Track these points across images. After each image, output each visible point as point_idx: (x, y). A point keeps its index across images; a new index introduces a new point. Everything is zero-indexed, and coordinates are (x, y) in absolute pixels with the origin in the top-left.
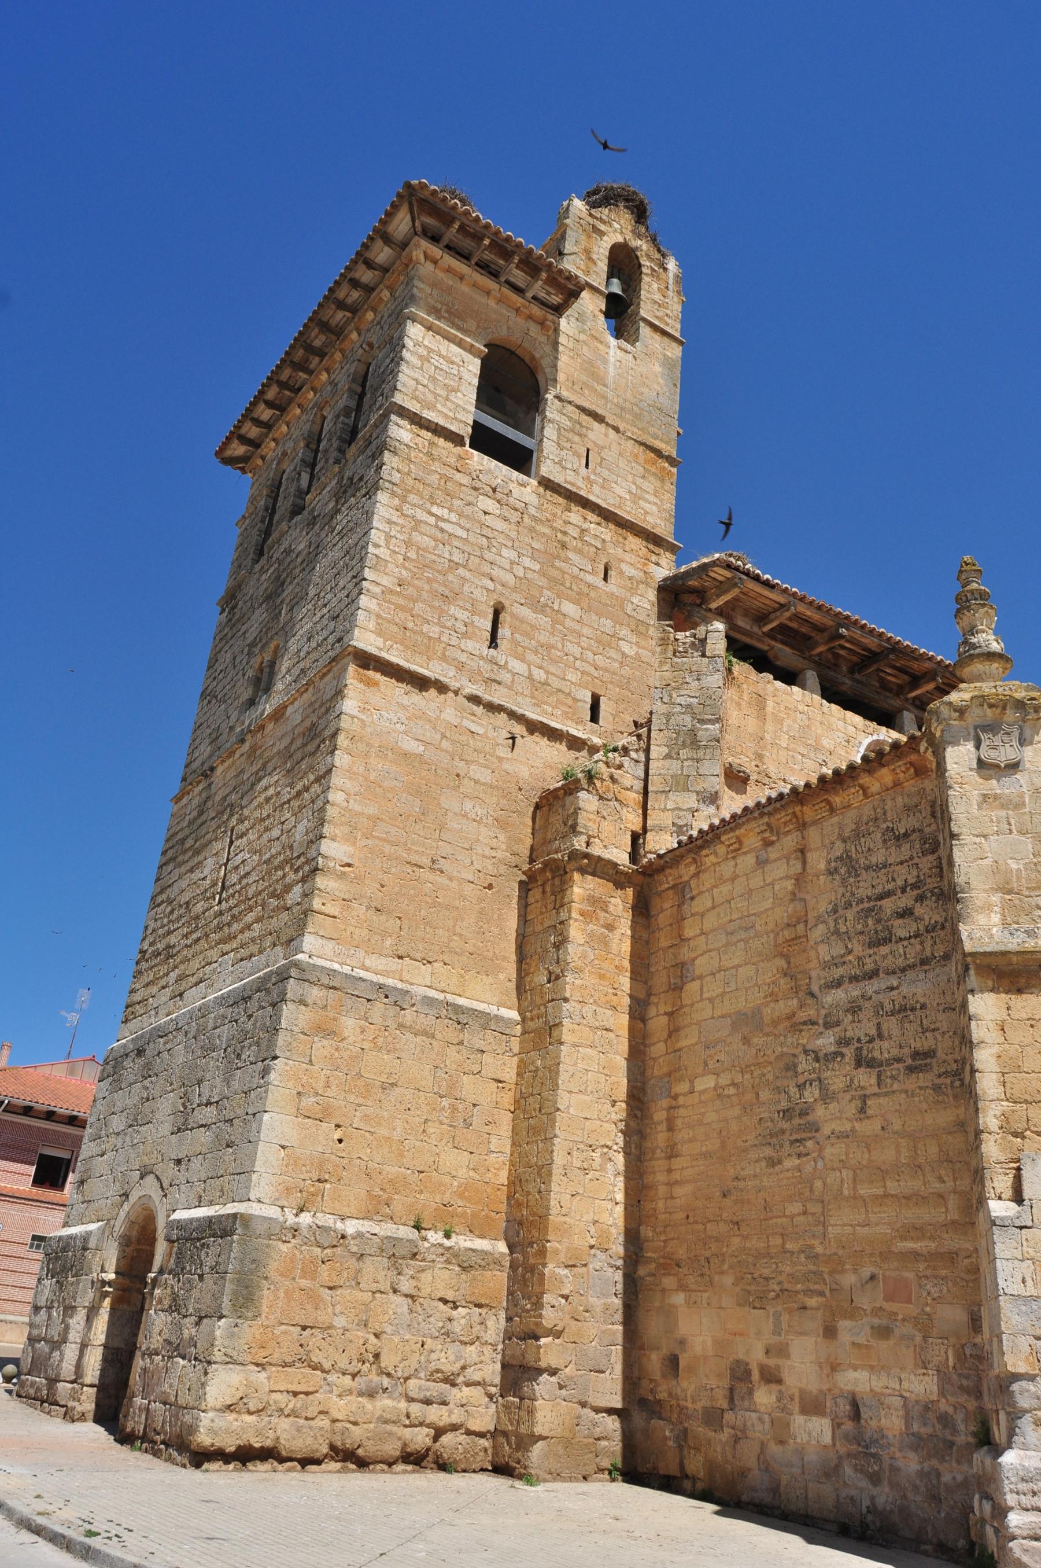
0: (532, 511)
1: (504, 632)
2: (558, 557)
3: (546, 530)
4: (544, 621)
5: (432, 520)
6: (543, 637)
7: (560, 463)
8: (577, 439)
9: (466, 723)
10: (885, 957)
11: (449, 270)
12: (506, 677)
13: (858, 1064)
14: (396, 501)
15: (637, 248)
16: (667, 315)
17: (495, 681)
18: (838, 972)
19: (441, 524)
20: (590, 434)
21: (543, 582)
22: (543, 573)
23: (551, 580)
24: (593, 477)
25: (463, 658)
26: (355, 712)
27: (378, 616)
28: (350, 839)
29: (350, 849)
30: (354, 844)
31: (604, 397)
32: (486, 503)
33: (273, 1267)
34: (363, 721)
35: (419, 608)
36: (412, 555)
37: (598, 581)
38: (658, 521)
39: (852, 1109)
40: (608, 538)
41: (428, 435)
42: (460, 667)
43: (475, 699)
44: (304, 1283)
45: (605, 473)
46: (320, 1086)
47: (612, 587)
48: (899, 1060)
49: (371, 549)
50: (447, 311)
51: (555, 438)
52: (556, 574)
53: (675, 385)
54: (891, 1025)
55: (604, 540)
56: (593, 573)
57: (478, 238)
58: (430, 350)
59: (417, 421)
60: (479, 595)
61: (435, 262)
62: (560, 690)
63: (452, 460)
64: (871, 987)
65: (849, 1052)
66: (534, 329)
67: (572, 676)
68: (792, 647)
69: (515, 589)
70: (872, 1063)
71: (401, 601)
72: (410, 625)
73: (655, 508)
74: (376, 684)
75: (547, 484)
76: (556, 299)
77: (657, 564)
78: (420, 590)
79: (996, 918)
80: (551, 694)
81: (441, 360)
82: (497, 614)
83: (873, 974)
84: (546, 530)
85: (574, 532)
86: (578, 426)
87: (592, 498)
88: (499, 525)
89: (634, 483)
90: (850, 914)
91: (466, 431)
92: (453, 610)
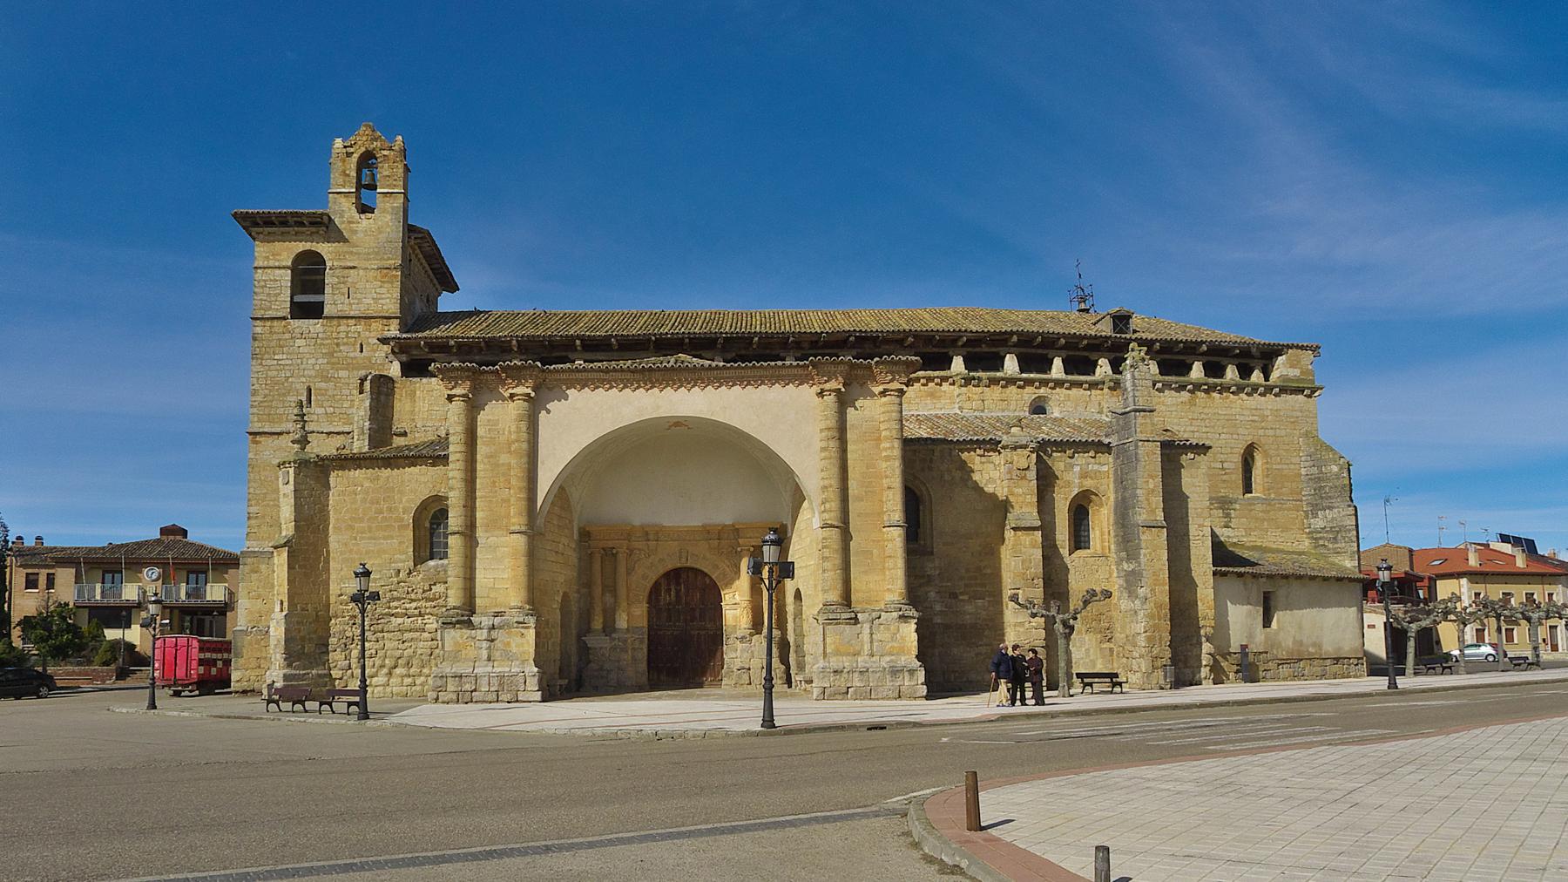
0: (320, 335)
2: (336, 352)
3: (328, 342)
6: (330, 393)
7: (334, 303)
8: (342, 286)
14: (260, 361)
20: (349, 280)
23: (333, 364)
24: (352, 302)
31: (359, 254)
32: (299, 342)
36: (269, 382)
37: (358, 354)
41: (268, 323)
50: (273, 255)
55: (359, 332)
56: (355, 351)
58: (265, 281)
68: (443, 353)
69: (315, 377)
71: (266, 404)
74: (260, 442)
77: (389, 330)
80: (336, 416)
82: (309, 390)
84: (329, 341)
85: (342, 335)
91: (286, 312)
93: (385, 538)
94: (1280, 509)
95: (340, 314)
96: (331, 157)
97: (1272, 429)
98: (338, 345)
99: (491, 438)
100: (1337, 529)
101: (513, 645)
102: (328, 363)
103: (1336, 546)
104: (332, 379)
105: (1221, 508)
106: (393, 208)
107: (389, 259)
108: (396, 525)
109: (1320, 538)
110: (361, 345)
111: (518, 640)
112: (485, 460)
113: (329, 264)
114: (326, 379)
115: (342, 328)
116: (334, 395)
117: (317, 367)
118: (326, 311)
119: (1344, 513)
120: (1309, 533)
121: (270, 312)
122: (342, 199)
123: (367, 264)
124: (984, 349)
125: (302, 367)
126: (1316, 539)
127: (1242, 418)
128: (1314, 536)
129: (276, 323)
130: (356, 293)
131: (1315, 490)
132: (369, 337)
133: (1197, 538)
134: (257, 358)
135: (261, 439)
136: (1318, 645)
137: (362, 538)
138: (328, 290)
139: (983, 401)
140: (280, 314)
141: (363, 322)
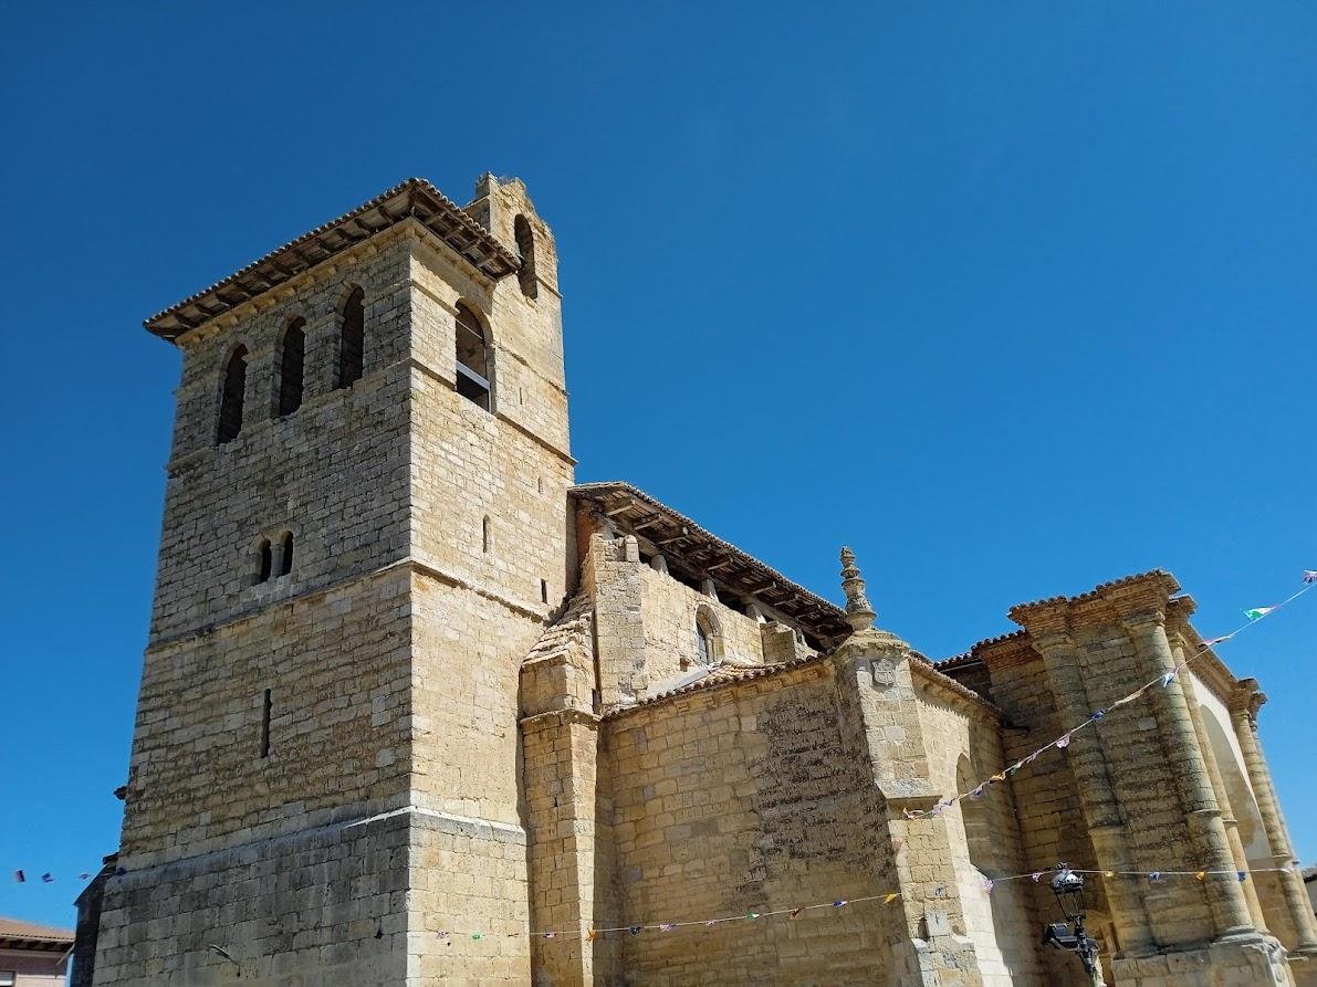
1: (491, 538)
2: (513, 477)
8: (514, 381)
9: (479, 613)
10: (805, 789)
11: (431, 245)
12: (495, 574)
13: (793, 855)
17: (490, 577)
18: (772, 798)
19: (449, 457)
25: (472, 562)
29: (428, 721)
30: (429, 717)
35: (444, 525)
37: (534, 492)
39: (790, 885)
42: (471, 569)
43: (482, 594)
46: (434, 906)
48: (820, 854)
49: (412, 481)
54: (813, 831)
57: (455, 224)
59: (425, 371)
61: (421, 237)
63: (449, 404)
64: (796, 808)
65: (785, 849)
66: (481, 290)
70: (802, 856)
75: (502, 418)
76: (498, 269)
79: (892, 776)
83: (798, 799)
87: (525, 427)
88: (479, 453)
90: (778, 760)
91: (453, 379)
114: (508, 517)
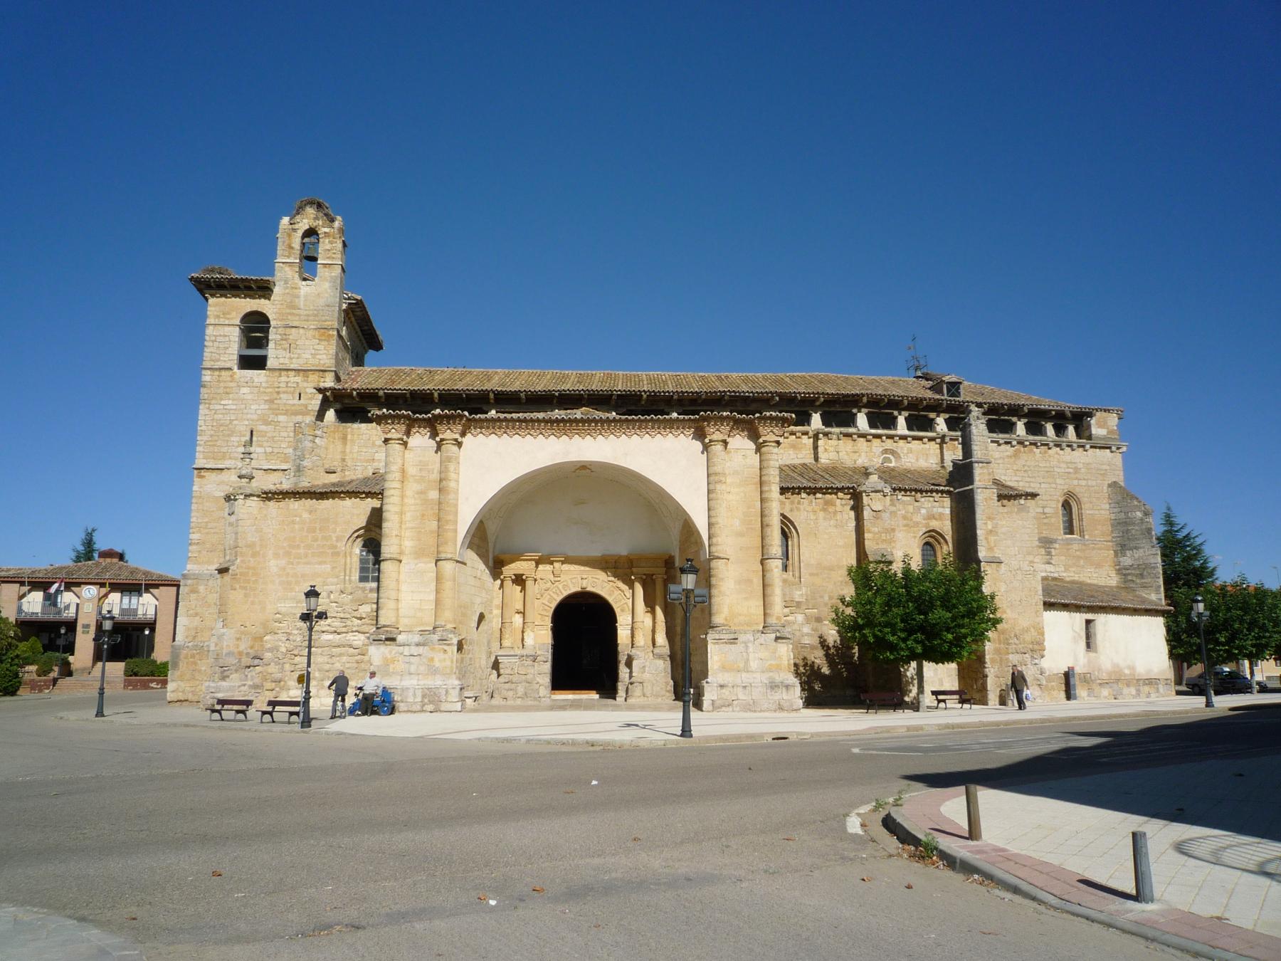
0: (264, 385)
1: (254, 439)
2: (276, 399)
3: (271, 390)
4: (270, 428)
5: (222, 407)
7: (277, 357)
8: (284, 342)
14: (207, 405)
15: (316, 227)
16: (334, 253)
19: (225, 407)
20: (291, 337)
21: (271, 412)
22: (270, 409)
26: (197, 489)
27: (204, 452)
28: (199, 532)
31: (299, 315)
33: (182, 657)
34: (200, 492)
35: (218, 443)
36: (215, 424)
37: (296, 401)
38: (327, 361)
40: (299, 381)
41: (217, 373)
44: (192, 660)
45: (299, 351)
46: (194, 607)
47: (302, 401)
49: (199, 428)
51: (274, 347)
52: (275, 406)
53: (337, 289)
55: (298, 383)
58: (216, 336)
60: (242, 428)
62: (278, 453)
67: (283, 445)
72: (216, 451)
73: (324, 356)
74: (203, 477)
77: (324, 382)
78: (218, 436)
80: (274, 456)
81: (221, 338)
82: (252, 432)
84: (271, 390)
85: (283, 385)
86: (284, 336)
88: (250, 397)
89: (313, 349)
92: (232, 439)
93: (320, 563)
94: (1093, 549)
95: (281, 367)
96: (278, 232)
97: (1084, 479)
98: (278, 393)
99: (421, 476)
100: (1144, 567)
101: (436, 660)
102: (270, 409)
103: (1143, 581)
104: (272, 423)
105: (1043, 547)
106: (331, 277)
107: (325, 321)
108: (330, 551)
109: (1129, 574)
110: (300, 394)
111: (442, 656)
112: (416, 496)
113: (272, 323)
114: (267, 423)
115: (283, 379)
116: (273, 437)
117: (259, 412)
118: (270, 363)
119: (1150, 552)
120: (1119, 570)
121: (219, 363)
122: (287, 268)
123: (305, 325)
124: (838, 408)
125: (245, 411)
126: (1125, 575)
127: (1059, 470)
128: (1122, 571)
129: (223, 373)
130: (296, 349)
131: (1123, 533)
132: (305, 388)
133: (1028, 573)
134: (205, 403)
135: (205, 474)
136: (1132, 668)
137: (298, 563)
138: (271, 345)
139: (838, 452)
140: (228, 365)
141: (301, 374)
